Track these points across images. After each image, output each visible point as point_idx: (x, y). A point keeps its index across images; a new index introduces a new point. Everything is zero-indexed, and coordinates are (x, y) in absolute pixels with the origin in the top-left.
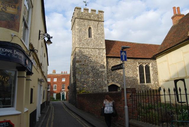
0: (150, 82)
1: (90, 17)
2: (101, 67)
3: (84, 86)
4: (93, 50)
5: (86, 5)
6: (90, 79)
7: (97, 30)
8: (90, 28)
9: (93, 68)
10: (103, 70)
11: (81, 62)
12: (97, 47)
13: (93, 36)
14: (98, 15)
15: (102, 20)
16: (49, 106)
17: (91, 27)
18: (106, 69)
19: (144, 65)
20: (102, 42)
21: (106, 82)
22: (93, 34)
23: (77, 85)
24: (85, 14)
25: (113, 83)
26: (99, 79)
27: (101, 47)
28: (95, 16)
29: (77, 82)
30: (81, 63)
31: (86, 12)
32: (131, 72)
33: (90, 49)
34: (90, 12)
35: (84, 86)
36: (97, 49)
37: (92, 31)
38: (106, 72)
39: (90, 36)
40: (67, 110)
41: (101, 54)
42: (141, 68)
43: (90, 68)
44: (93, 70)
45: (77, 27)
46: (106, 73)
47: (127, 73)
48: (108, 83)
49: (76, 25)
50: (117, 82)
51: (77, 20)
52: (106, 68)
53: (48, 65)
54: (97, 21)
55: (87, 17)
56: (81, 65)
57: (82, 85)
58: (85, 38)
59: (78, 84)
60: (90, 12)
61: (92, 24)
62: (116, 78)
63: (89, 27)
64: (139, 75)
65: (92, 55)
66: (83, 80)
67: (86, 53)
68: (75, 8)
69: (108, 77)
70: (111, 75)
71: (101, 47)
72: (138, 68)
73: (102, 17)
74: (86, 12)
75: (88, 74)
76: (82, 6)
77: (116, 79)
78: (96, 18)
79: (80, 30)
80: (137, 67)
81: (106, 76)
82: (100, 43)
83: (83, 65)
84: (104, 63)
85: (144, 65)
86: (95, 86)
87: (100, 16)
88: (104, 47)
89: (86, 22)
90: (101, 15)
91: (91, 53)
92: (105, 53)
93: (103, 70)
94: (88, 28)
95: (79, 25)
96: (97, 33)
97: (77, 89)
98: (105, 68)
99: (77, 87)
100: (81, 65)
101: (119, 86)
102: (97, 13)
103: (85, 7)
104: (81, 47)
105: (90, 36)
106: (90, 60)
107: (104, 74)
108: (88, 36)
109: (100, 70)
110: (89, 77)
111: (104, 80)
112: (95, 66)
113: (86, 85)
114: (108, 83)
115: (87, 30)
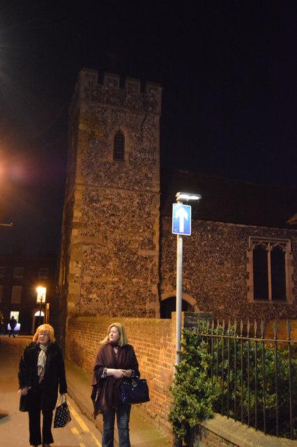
0: (285, 299)
2: (143, 245)
3: (90, 296)
7: (140, 139)
9: (121, 248)
10: (151, 253)
13: (126, 157)
18: (156, 253)
19: (269, 248)
21: (155, 289)
22: (126, 149)
23: (71, 291)
26: (134, 280)
29: (70, 284)
32: (229, 265)
35: (90, 296)
37: (127, 141)
38: (156, 260)
41: (147, 209)
42: (259, 254)
43: (111, 245)
44: (119, 250)
46: (157, 264)
47: (216, 266)
52: (157, 248)
57: (85, 293)
64: (251, 276)
65: (121, 208)
67: (103, 203)
72: (250, 255)
80: (249, 251)
82: (146, 175)
84: (153, 234)
85: (269, 248)
86: (124, 296)
87: (152, 99)
88: (158, 189)
92: (158, 206)
93: (151, 253)
98: (153, 248)
105: (119, 154)
106: (114, 222)
107: (150, 266)
108: (111, 158)
109: (143, 253)
110: (108, 272)
111: (149, 282)
112: (127, 243)
114: (160, 292)
115: (111, 137)
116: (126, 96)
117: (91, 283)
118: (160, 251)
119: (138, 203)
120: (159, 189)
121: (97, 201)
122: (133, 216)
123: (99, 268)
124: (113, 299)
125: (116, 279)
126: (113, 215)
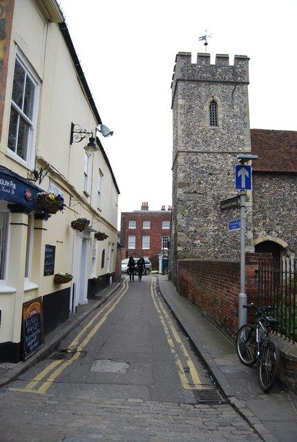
1: (214, 75)
3: (195, 242)
4: (219, 156)
5: (206, 44)
6: (211, 227)
7: (231, 106)
8: (214, 103)
11: (188, 185)
12: (230, 150)
13: (220, 123)
14: (233, 67)
15: (245, 81)
16: (119, 284)
17: (216, 98)
20: (242, 137)
21: (250, 235)
22: (220, 116)
23: (179, 239)
24: (200, 69)
25: (269, 238)
27: (240, 149)
28: (226, 72)
30: (188, 189)
31: (204, 63)
33: (212, 155)
34: (213, 61)
35: (195, 242)
36: (230, 153)
37: (220, 109)
39: (214, 121)
40: (153, 294)
45: (181, 102)
46: (251, 214)
48: (255, 236)
49: (180, 96)
50: (278, 236)
51: (181, 84)
52: (251, 200)
53: (119, 193)
54: (232, 83)
55: (205, 75)
56: (189, 193)
58: (201, 128)
59: (182, 238)
60: (213, 61)
61: (218, 92)
62: (278, 224)
63: (211, 99)
65: (218, 167)
66: (192, 229)
67: (202, 165)
68: (177, 55)
69: (255, 223)
70: (264, 218)
71: (240, 149)
73: (245, 73)
74: (204, 63)
75: (206, 213)
76: (195, 49)
77: (278, 228)
78: (229, 77)
79: (190, 109)
81: (250, 221)
83: (195, 192)
89: (203, 90)
90: (241, 67)
91: (214, 165)
94: (208, 103)
95: (188, 97)
96: (231, 114)
97: (179, 249)
99: (179, 245)
100: (189, 193)
101: (285, 245)
102: (231, 62)
103: (203, 50)
104: (190, 149)
105: (214, 121)
110: (209, 222)
113: (199, 241)
114: (255, 236)
115: (207, 108)
116: (217, 71)
117: (196, 231)
118: (254, 202)
119: (232, 162)
120: (250, 149)
121: (196, 164)
122: (229, 174)
123: (202, 220)
124: (214, 244)
125: (216, 228)
126: (211, 174)
